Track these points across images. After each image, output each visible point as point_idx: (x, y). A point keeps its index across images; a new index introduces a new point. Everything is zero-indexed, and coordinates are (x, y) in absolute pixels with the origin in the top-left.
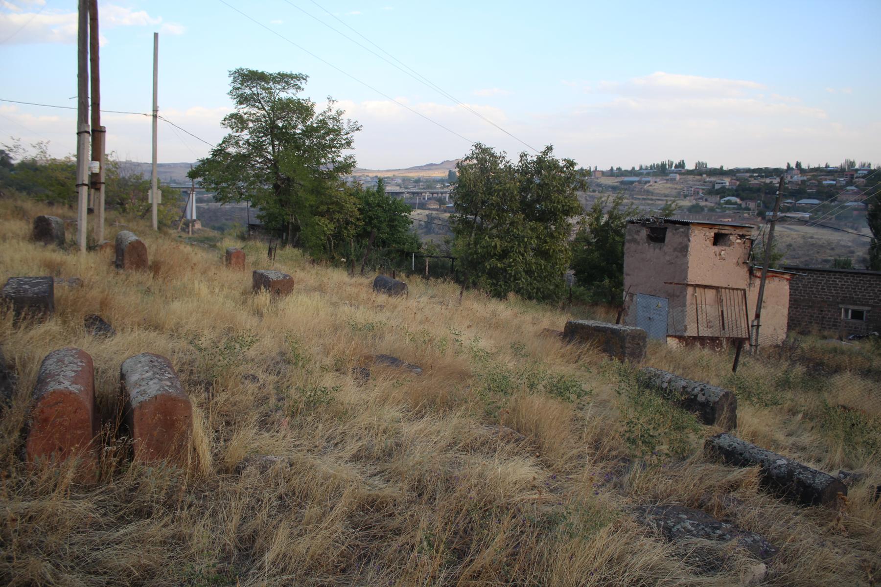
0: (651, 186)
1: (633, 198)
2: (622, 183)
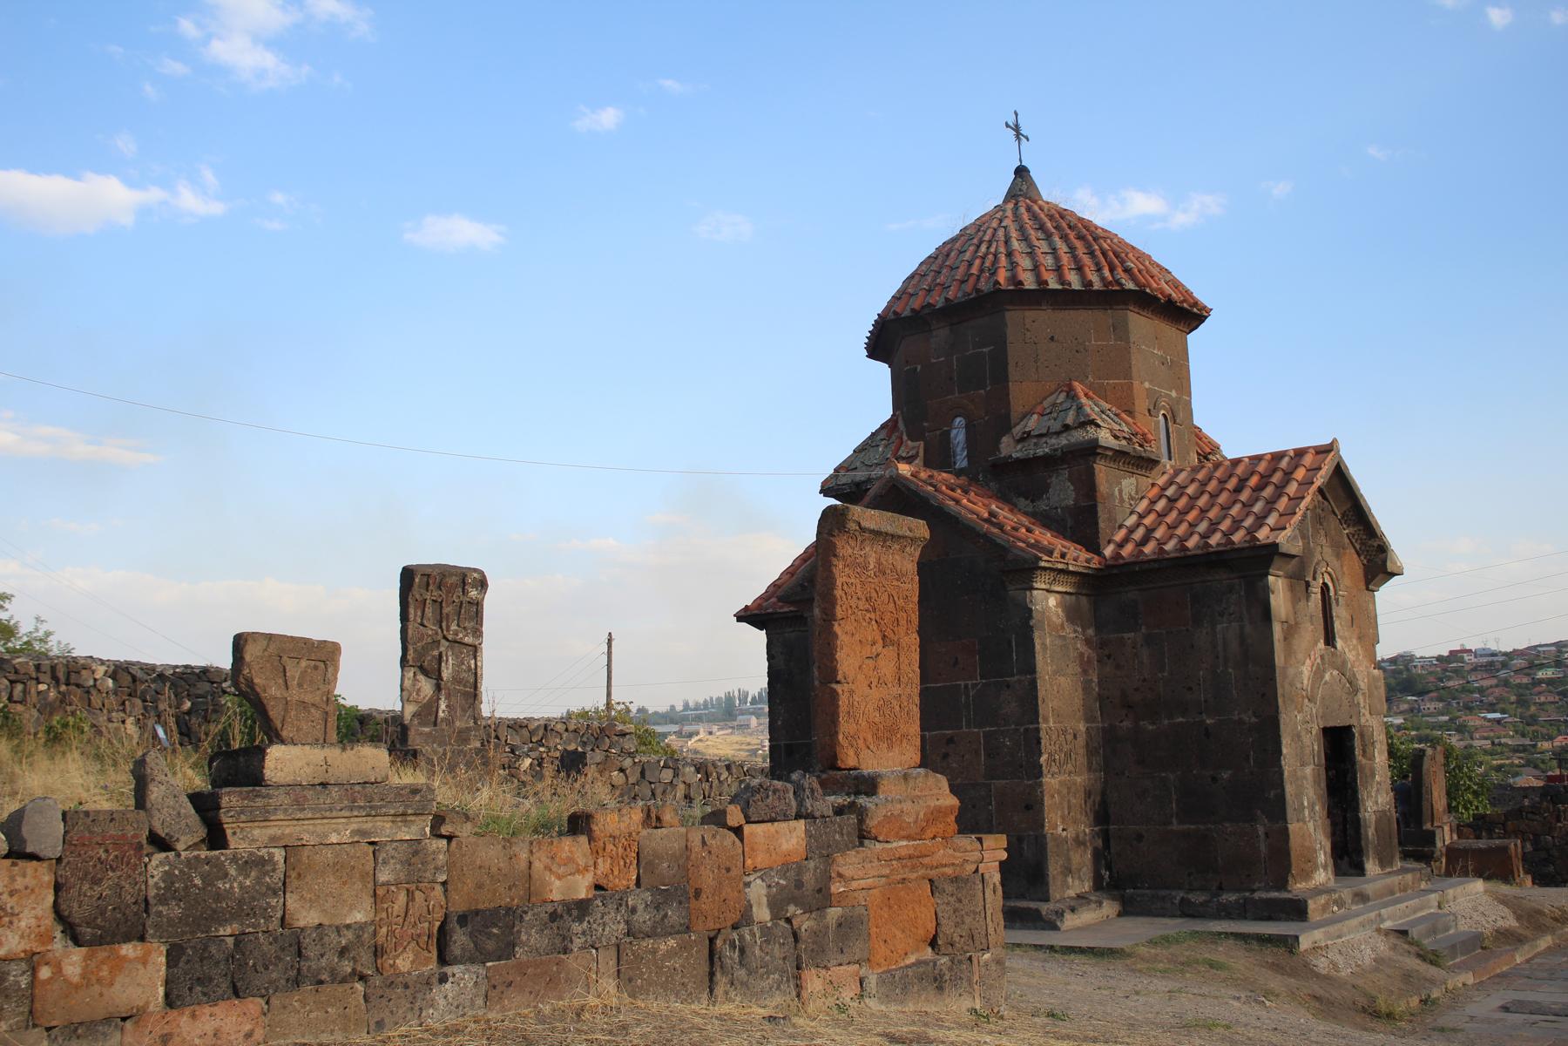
0: (700, 740)
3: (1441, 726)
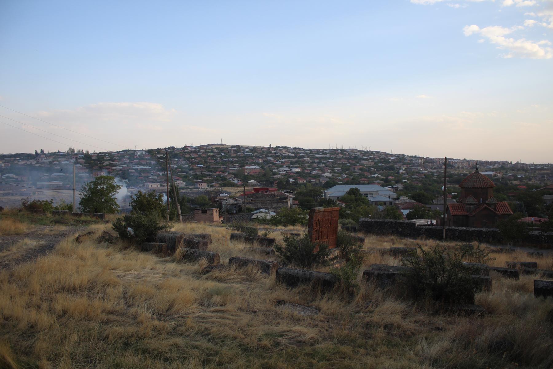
3: (187, 168)
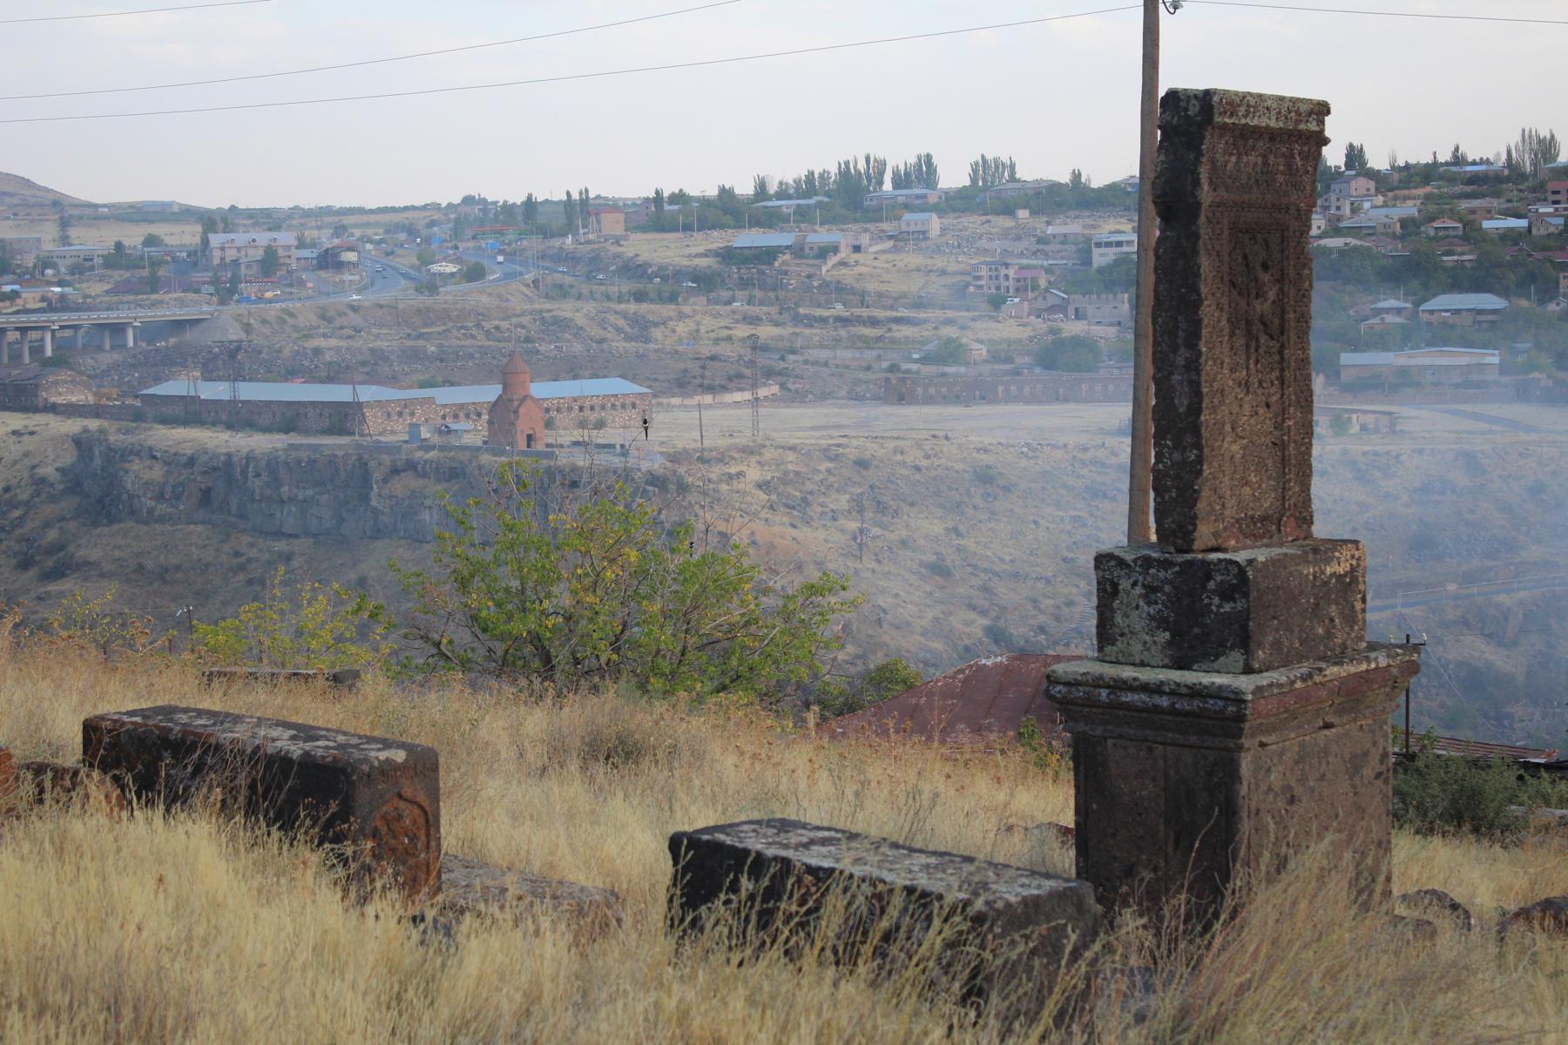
0: (843, 264)
1: (797, 319)
2: (728, 255)
